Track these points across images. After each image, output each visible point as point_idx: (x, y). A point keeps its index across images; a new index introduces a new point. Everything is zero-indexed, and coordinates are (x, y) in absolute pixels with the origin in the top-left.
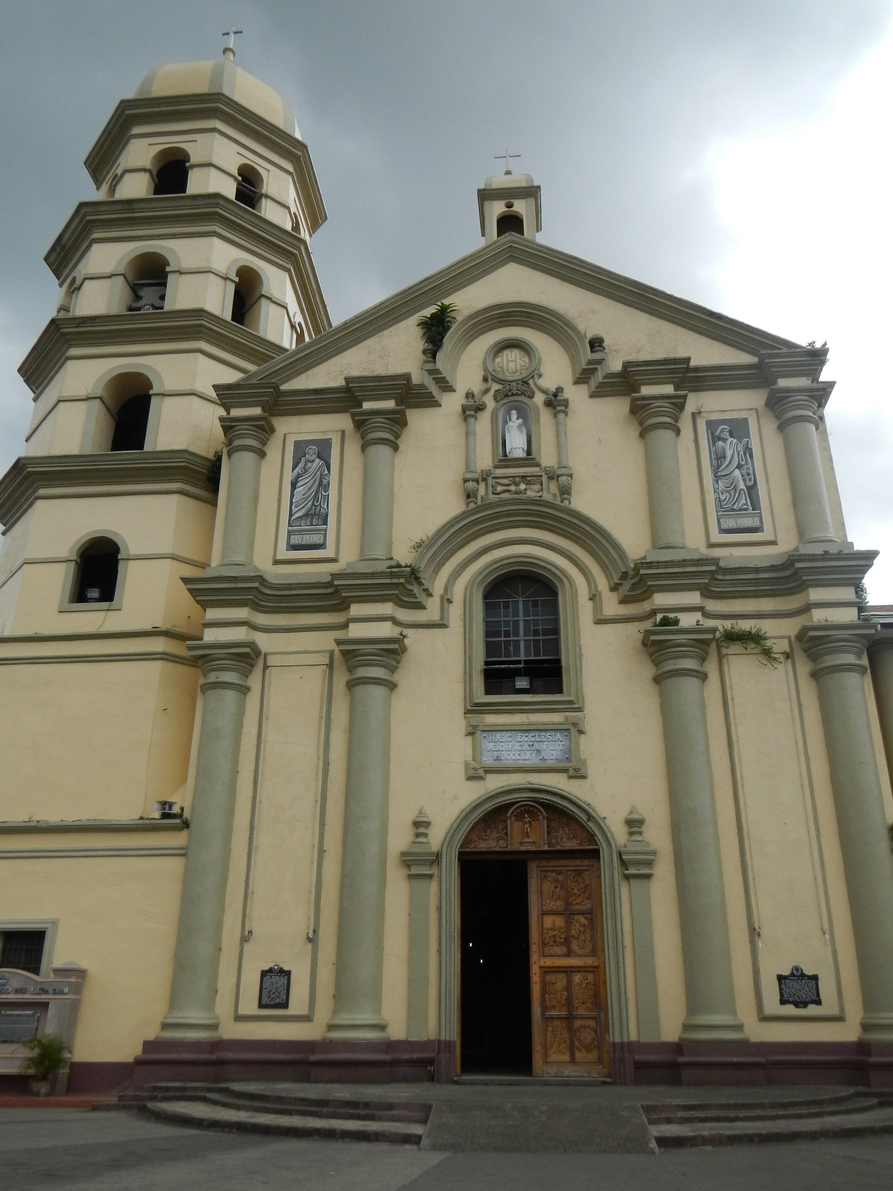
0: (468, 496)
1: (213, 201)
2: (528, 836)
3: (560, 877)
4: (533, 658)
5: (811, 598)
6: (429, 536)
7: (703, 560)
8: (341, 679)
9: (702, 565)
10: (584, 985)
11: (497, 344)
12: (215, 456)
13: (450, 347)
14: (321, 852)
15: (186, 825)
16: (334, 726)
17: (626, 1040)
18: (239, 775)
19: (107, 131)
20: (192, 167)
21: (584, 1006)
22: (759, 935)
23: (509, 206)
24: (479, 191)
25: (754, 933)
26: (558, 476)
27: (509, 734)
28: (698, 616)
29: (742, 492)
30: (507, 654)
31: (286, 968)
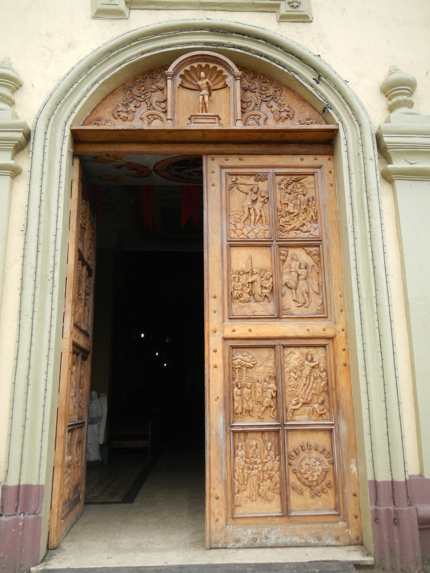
3: (263, 186)
10: (307, 371)
17: (400, 478)
21: (308, 408)
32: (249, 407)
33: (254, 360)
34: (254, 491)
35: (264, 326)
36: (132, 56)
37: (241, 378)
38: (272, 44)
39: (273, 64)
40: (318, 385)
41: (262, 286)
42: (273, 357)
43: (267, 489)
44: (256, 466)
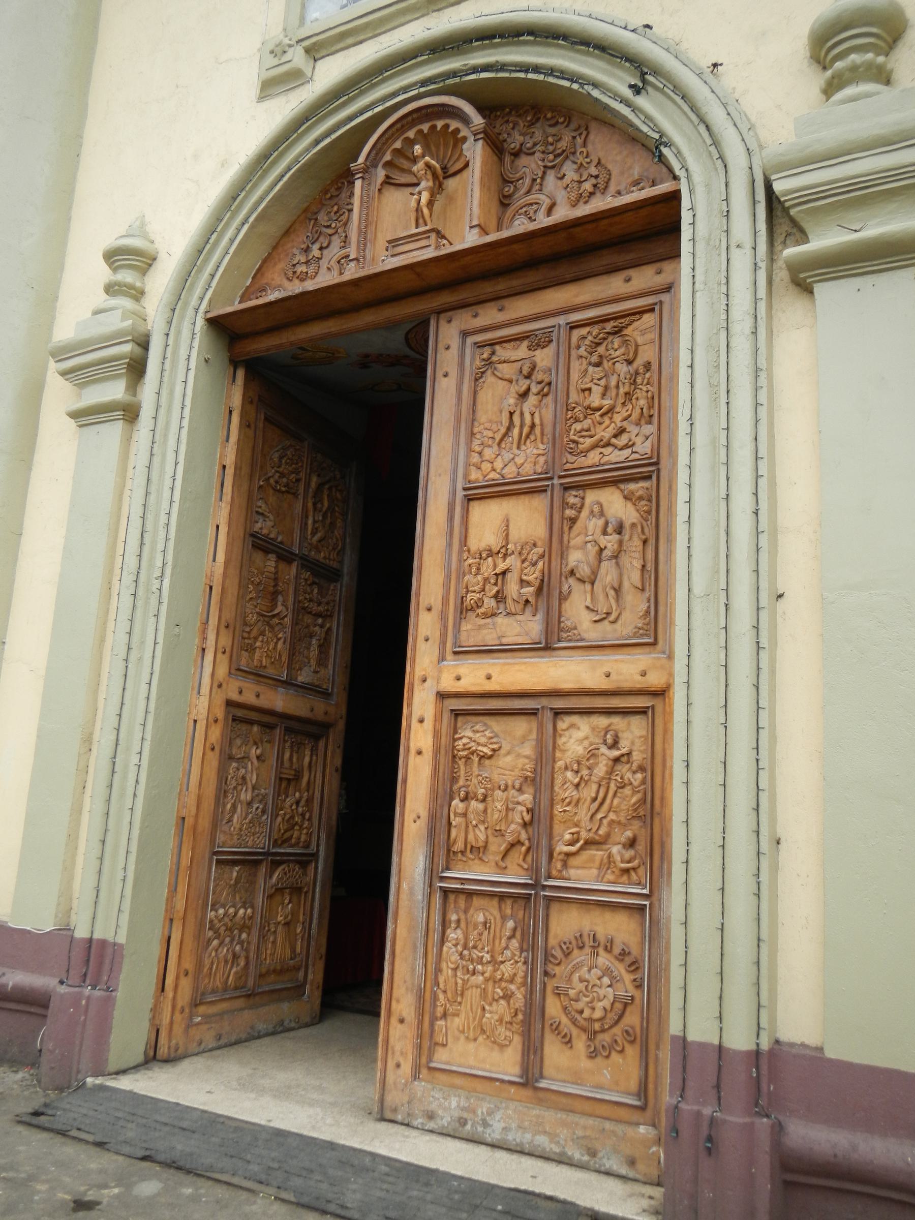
3: (544, 357)
10: (601, 770)
21: (598, 854)
32: (477, 841)
33: (494, 740)
34: (471, 1019)
35: (517, 667)
36: (301, 154)
37: (469, 778)
38: (547, 37)
39: (551, 80)
40: (625, 803)
41: (522, 581)
42: (534, 736)
43: (497, 1021)
44: (480, 967)
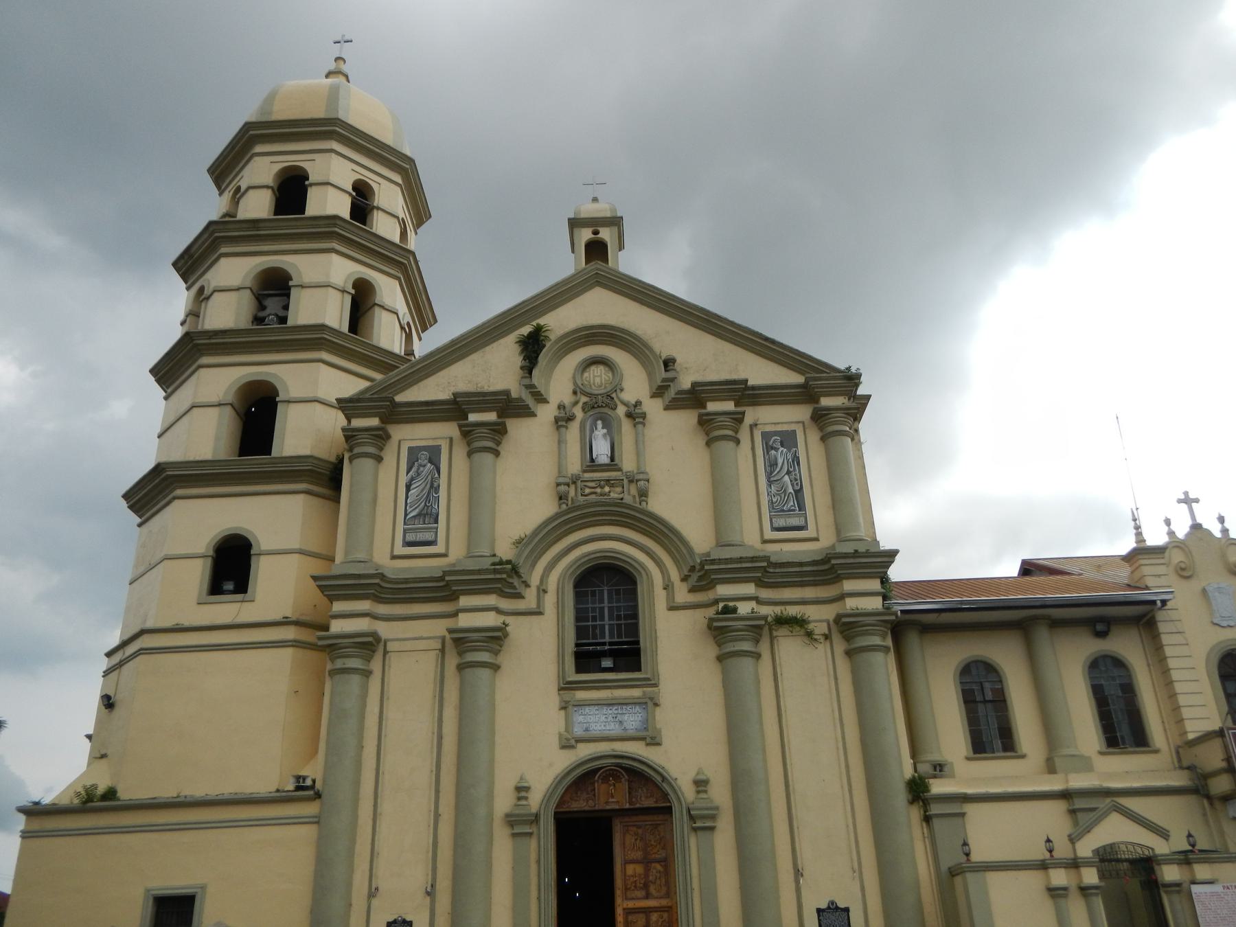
0: (560, 498)
1: (332, 222)
2: (612, 797)
3: (640, 831)
4: (616, 640)
5: (845, 589)
6: (527, 533)
7: (756, 557)
8: (452, 661)
9: (756, 561)
10: (660, 923)
11: (585, 361)
12: (337, 459)
13: (544, 364)
14: (437, 816)
15: (318, 795)
16: (446, 704)
18: (364, 749)
19: (231, 146)
20: (311, 185)
22: (802, 875)
23: (596, 233)
24: (569, 219)
25: (798, 873)
26: (637, 481)
27: (596, 708)
28: (753, 604)
29: (791, 495)
30: (595, 637)
31: (408, 919)
